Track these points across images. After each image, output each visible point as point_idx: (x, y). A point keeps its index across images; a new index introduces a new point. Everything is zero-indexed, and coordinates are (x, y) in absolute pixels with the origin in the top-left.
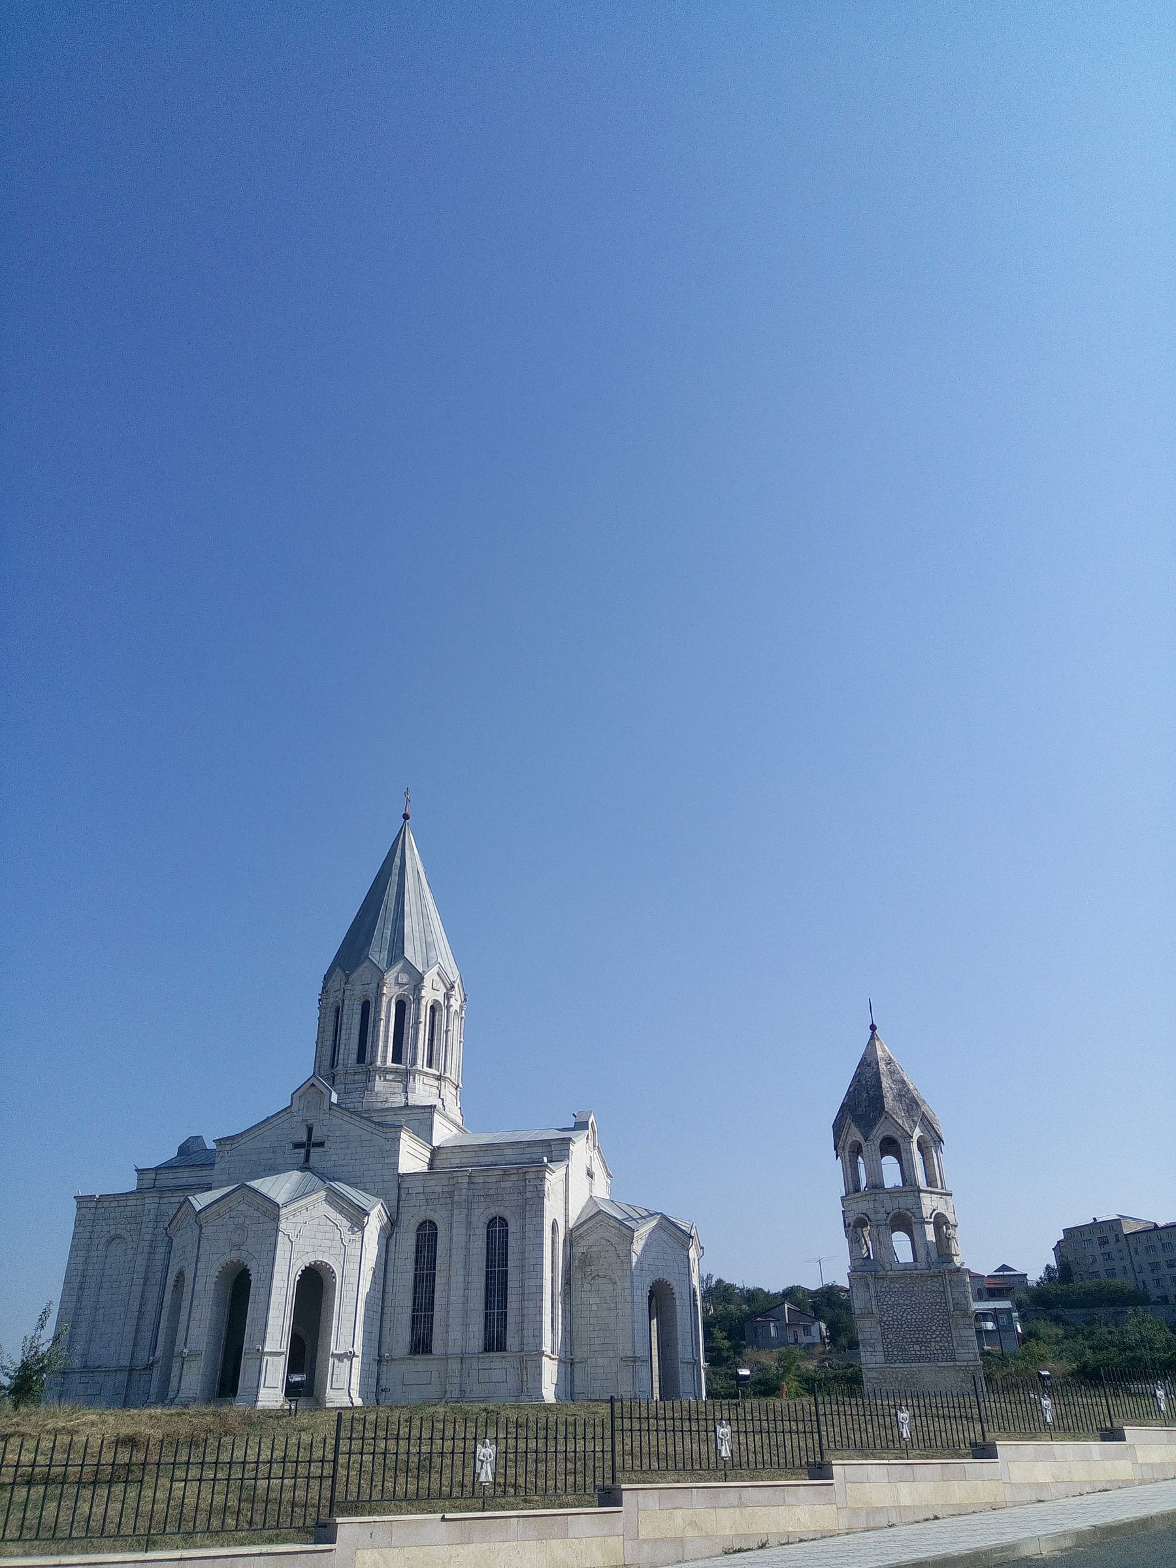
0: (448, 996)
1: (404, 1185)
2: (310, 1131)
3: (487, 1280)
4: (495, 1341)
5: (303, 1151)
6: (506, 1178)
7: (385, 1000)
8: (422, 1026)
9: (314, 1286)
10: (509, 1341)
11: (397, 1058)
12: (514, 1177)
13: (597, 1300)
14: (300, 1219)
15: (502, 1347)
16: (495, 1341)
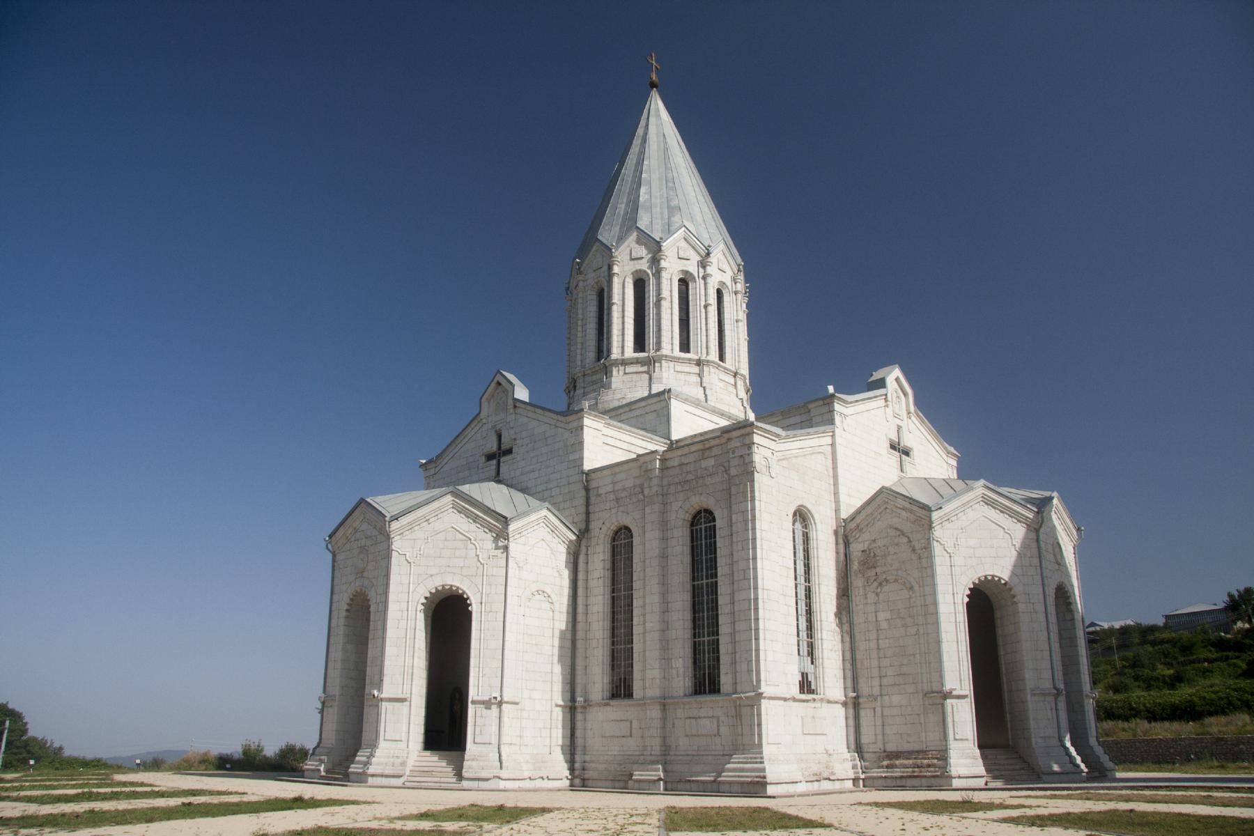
0: (703, 264)
1: (593, 485)
2: (499, 437)
3: (694, 597)
4: (706, 680)
5: (494, 462)
6: (707, 454)
7: (616, 282)
8: (665, 305)
9: (449, 619)
10: (723, 679)
11: (640, 344)
12: (716, 451)
13: (888, 615)
14: (419, 533)
15: (714, 688)
16: (706, 680)
